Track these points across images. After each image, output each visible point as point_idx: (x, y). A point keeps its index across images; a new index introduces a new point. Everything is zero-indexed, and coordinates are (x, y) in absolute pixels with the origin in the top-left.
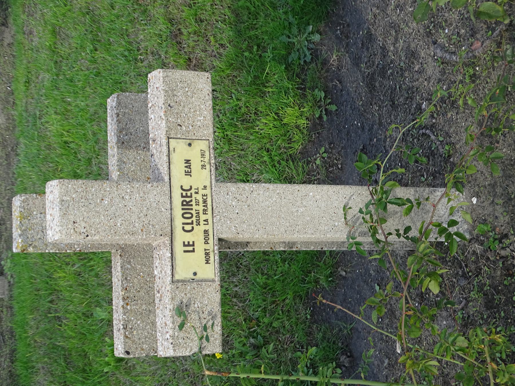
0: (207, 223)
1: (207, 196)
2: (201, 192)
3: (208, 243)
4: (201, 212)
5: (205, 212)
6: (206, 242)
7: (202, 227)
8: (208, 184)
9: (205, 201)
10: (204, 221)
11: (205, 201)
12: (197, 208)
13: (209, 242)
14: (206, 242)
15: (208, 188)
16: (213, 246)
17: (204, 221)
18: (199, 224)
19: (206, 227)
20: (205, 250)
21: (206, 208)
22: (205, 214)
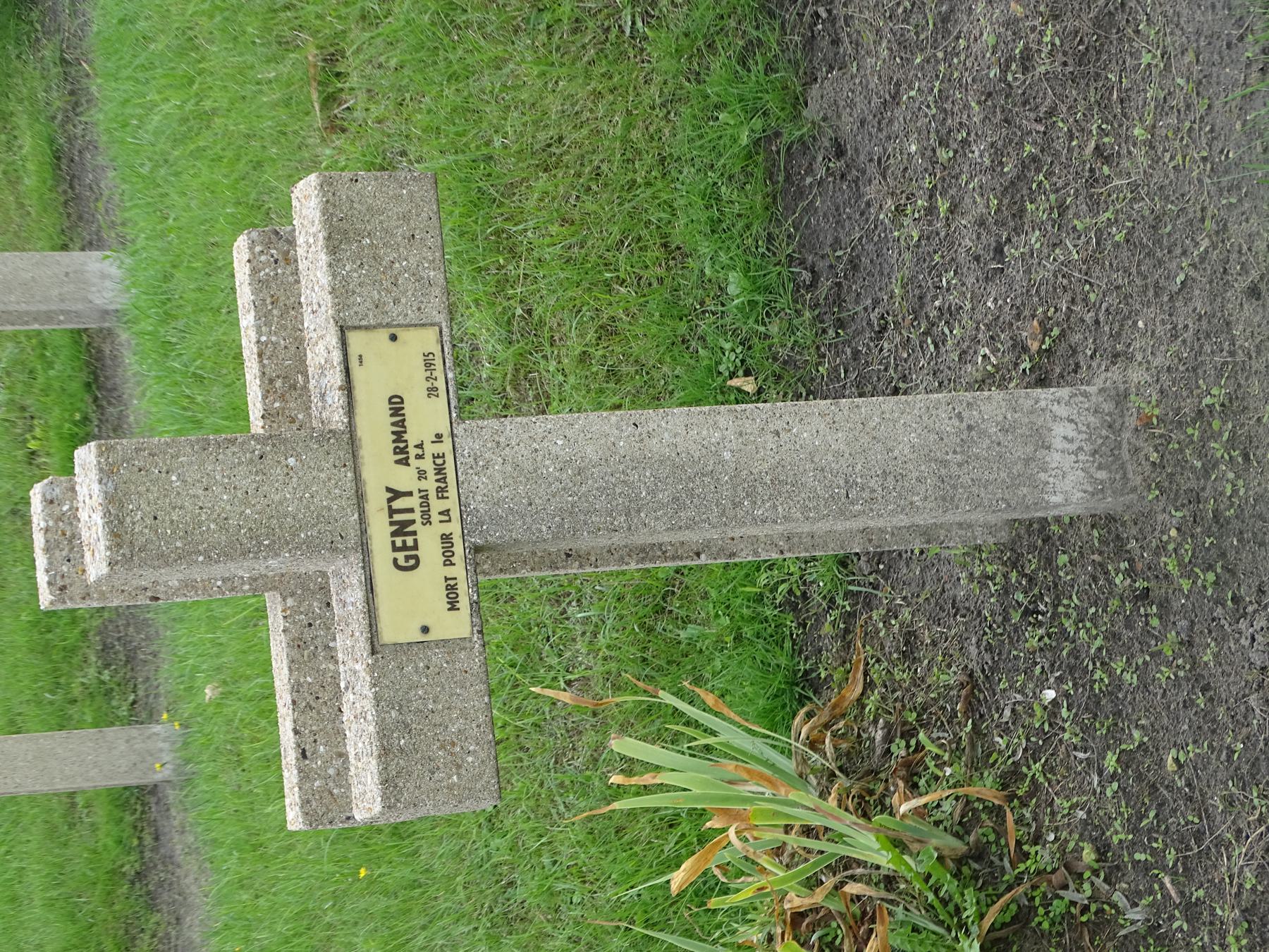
0: (447, 518)
1: (443, 456)
2: (430, 449)
4: (432, 495)
5: (441, 492)
7: (438, 528)
8: (444, 429)
9: (440, 470)
11: (440, 470)
12: (423, 485)
13: (453, 560)
14: (448, 562)
18: (427, 521)
19: (446, 528)
20: (446, 579)
22: (443, 498)
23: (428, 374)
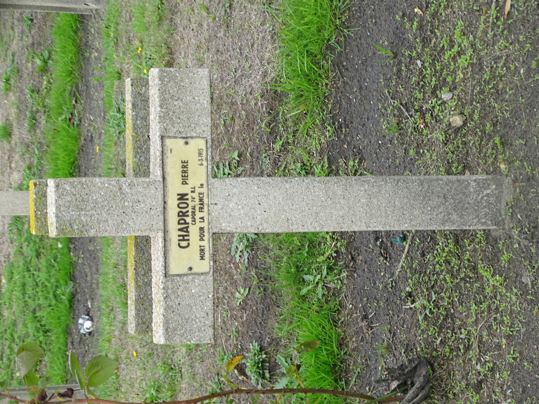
0: (202, 220)
1: (203, 194)
2: (198, 190)
3: (203, 240)
6: (202, 239)
7: (199, 225)
8: (204, 182)
9: (201, 200)
10: (200, 218)
11: (201, 200)
13: (204, 238)
14: (202, 239)
15: (205, 186)
16: (206, 244)
17: (200, 218)
19: (202, 225)
20: (200, 246)
21: (202, 206)
22: (202, 211)
23: (200, 158)
